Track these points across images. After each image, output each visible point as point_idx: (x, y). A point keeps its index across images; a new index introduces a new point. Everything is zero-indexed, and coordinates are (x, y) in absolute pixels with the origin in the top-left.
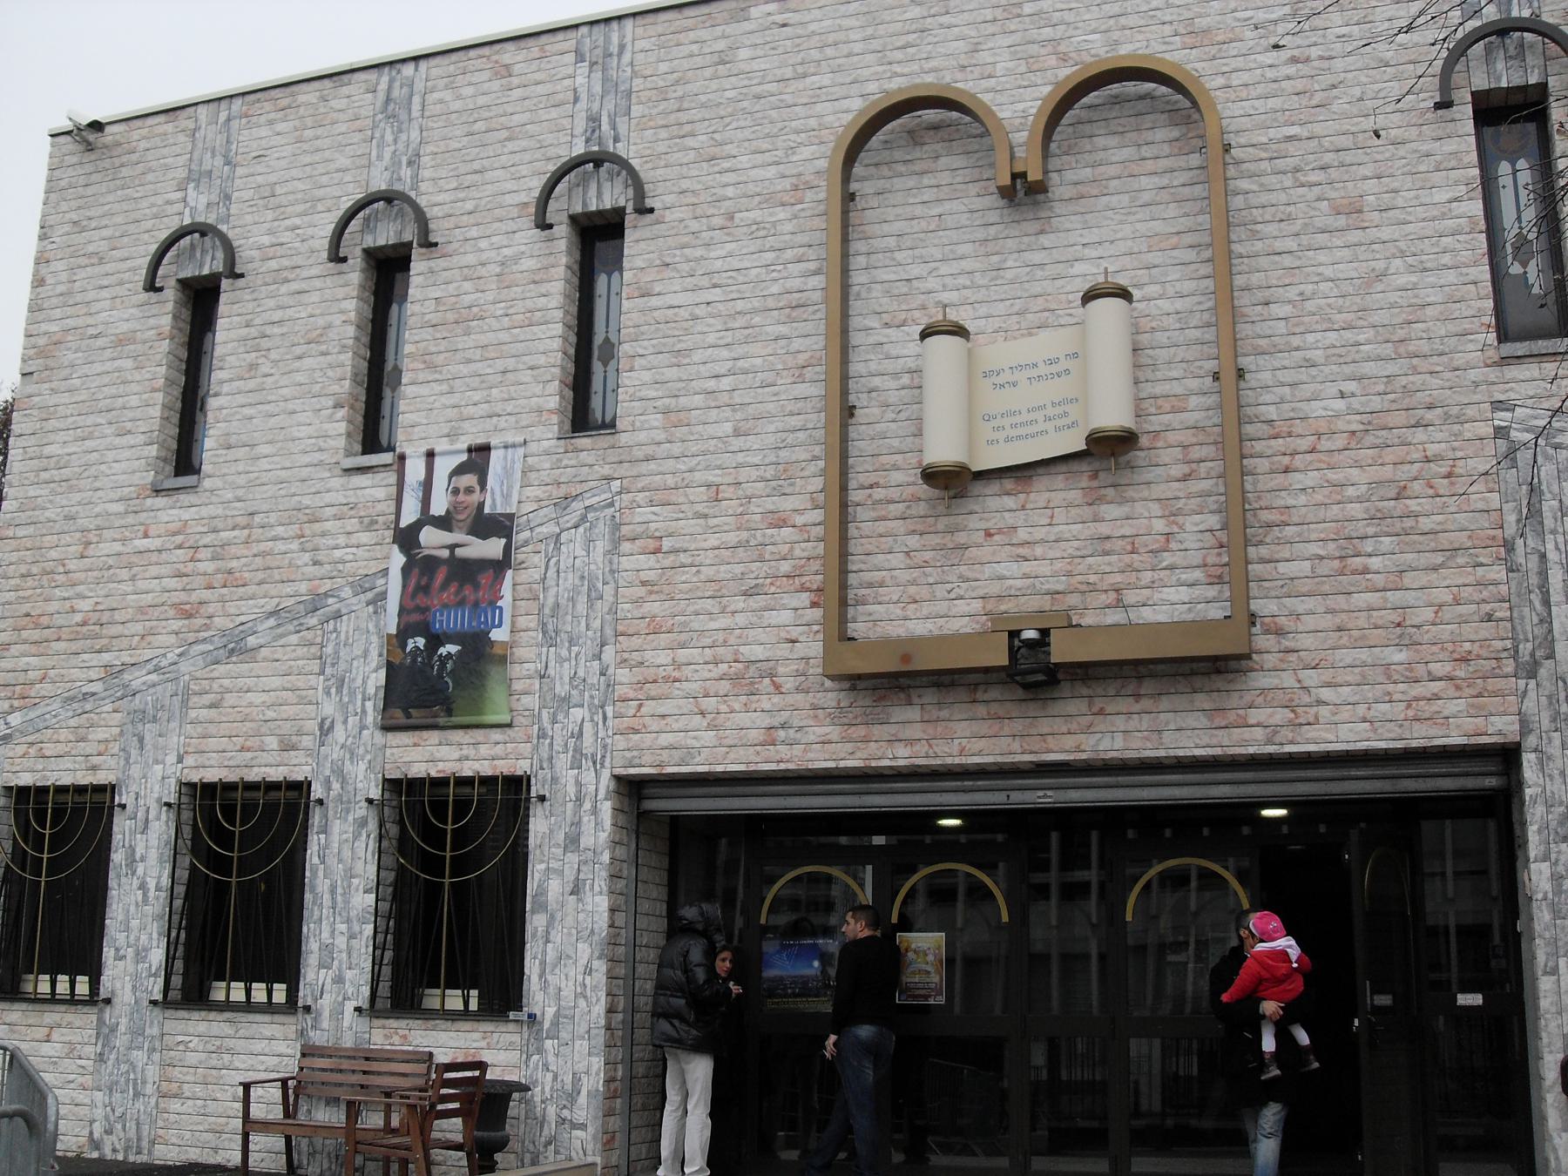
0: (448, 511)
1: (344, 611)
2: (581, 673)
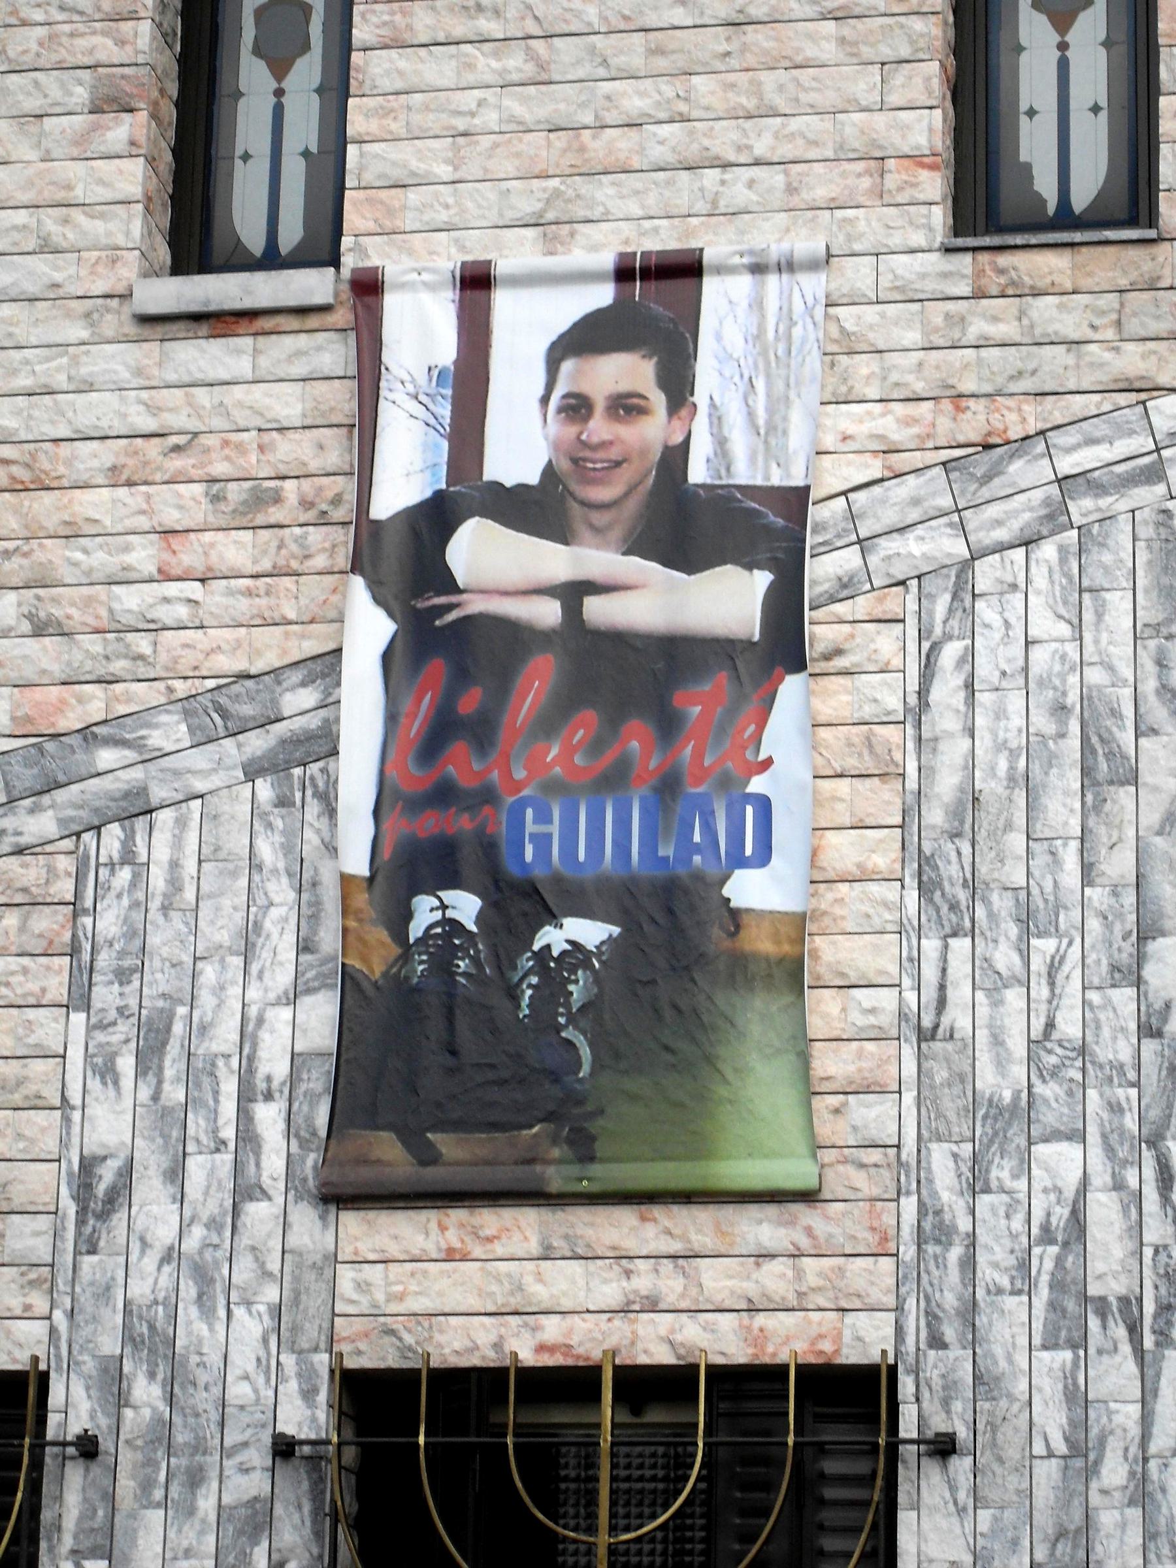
0: (549, 472)
1: (158, 793)
2: (1069, 1026)
